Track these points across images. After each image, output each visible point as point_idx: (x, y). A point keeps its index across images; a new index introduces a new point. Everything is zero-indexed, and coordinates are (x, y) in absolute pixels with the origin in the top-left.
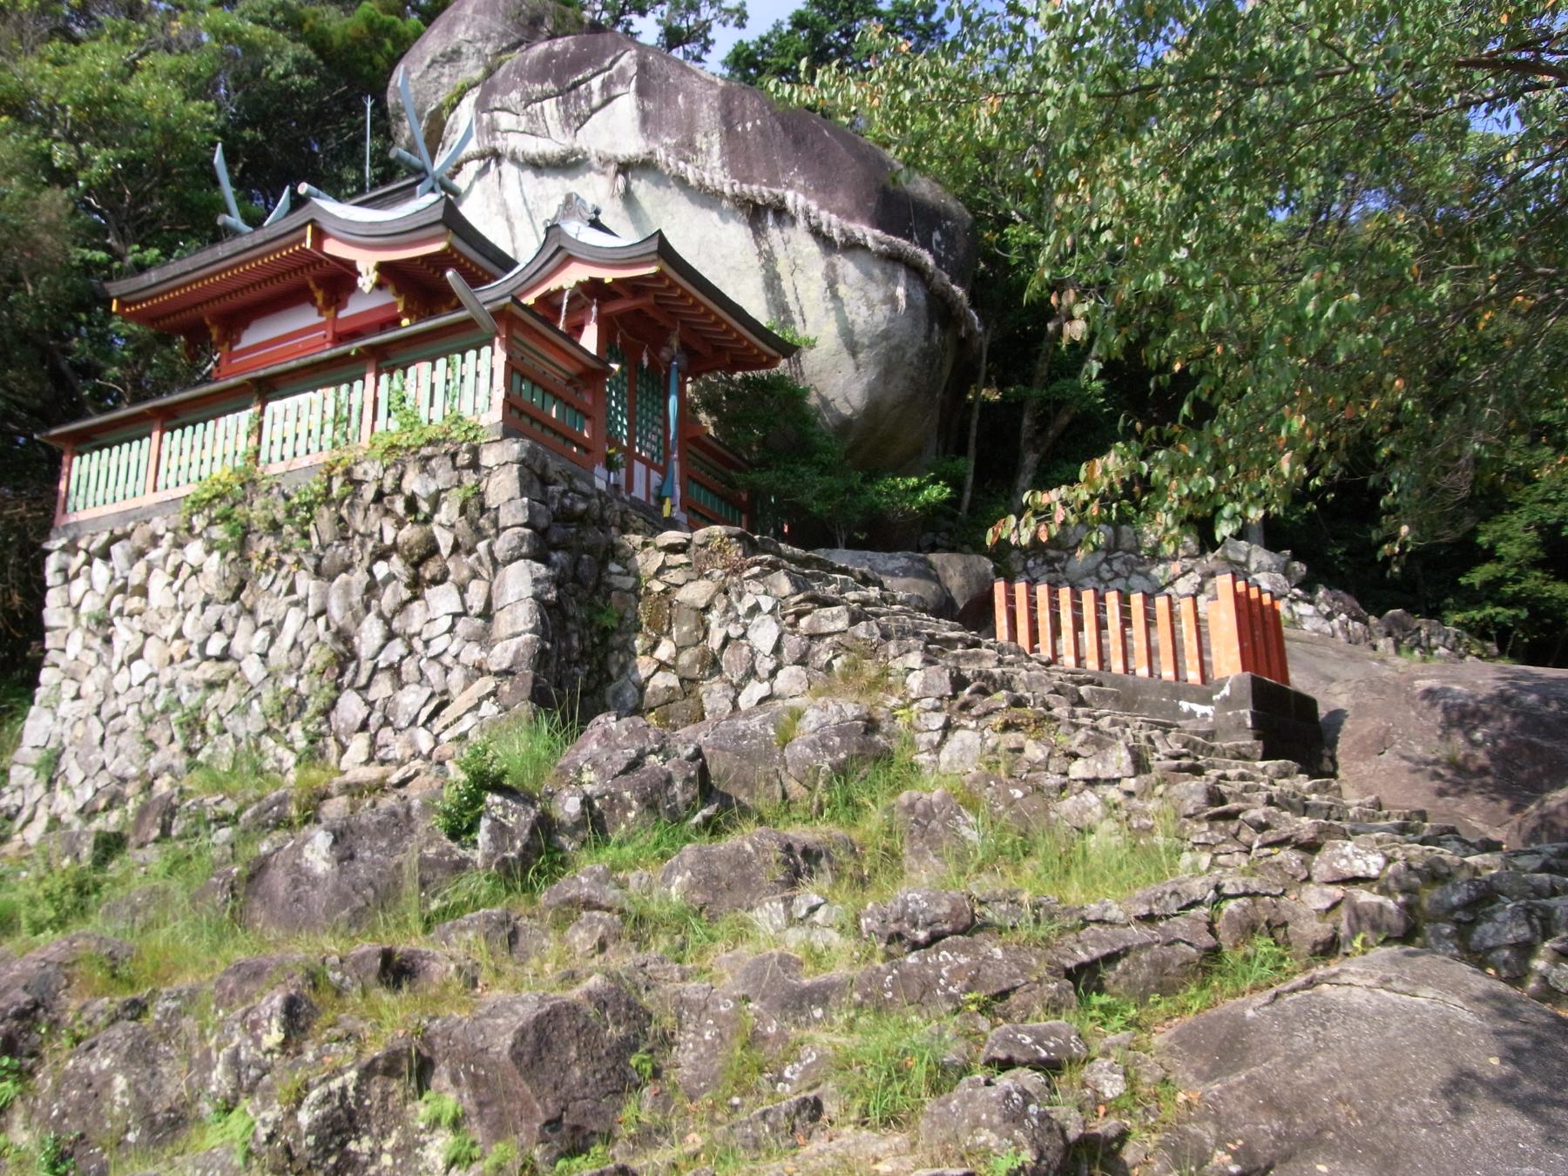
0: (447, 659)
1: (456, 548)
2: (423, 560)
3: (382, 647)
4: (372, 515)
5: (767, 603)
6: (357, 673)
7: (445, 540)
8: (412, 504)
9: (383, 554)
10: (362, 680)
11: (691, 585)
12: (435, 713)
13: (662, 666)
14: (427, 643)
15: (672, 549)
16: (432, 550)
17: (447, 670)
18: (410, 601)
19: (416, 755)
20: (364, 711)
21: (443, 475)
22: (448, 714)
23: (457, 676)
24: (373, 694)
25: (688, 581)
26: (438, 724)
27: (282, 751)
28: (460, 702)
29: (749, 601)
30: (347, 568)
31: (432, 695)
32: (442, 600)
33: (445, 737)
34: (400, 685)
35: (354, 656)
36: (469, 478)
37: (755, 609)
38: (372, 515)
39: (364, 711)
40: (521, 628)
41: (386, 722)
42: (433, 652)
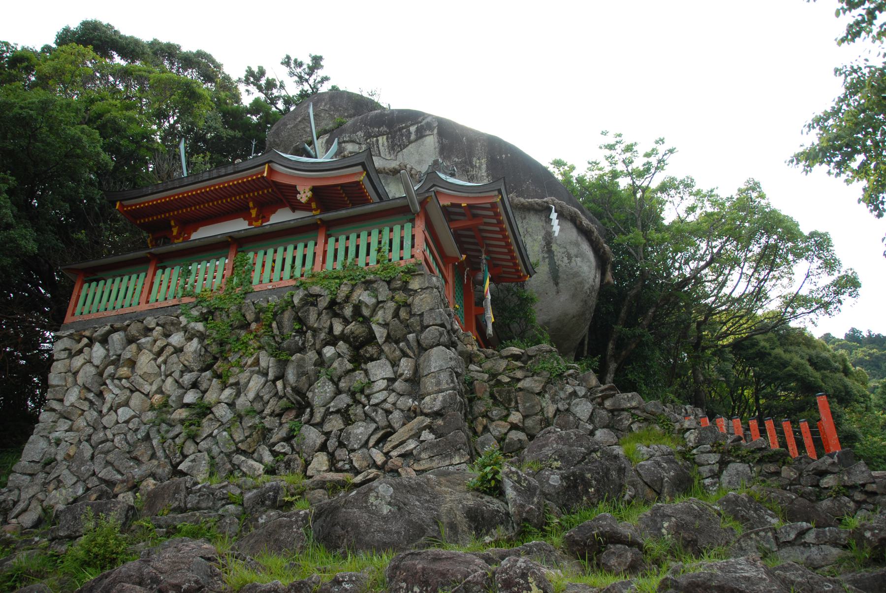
0: (387, 406)
1: (388, 338)
2: (363, 345)
3: (333, 398)
4: (324, 317)
5: (581, 391)
6: (312, 414)
7: (380, 333)
8: (357, 309)
9: (333, 341)
10: (318, 418)
11: (528, 380)
12: (383, 439)
13: (514, 427)
14: (368, 397)
15: (516, 357)
16: (371, 338)
17: (388, 412)
18: (353, 370)
19: (374, 465)
20: (323, 438)
21: (384, 292)
22: (394, 439)
23: (396, 415)
24: (327, 427)
25: (526, 377)
26: (388, 446)
27: (256, 465)
28: (402, 433)
29: (569, 389)
30: (302, 350)
31: (376, 430)
32: (380, 371)
33: (394, 453)
34: (348, 421)
35: (309, 404)
36: (400, 296)
37: (574, 394)
38: (324, 317)
39: (323, 438)
40: (445, 386)
41: (341, 445)
42: (374, 401)
